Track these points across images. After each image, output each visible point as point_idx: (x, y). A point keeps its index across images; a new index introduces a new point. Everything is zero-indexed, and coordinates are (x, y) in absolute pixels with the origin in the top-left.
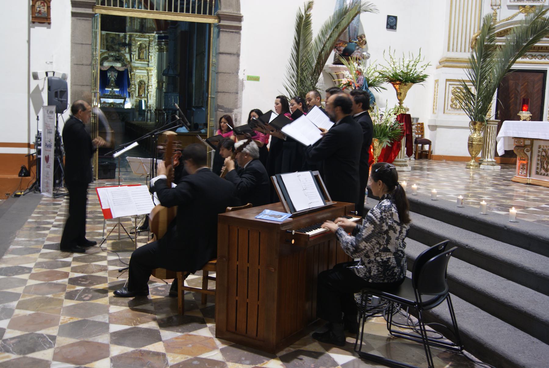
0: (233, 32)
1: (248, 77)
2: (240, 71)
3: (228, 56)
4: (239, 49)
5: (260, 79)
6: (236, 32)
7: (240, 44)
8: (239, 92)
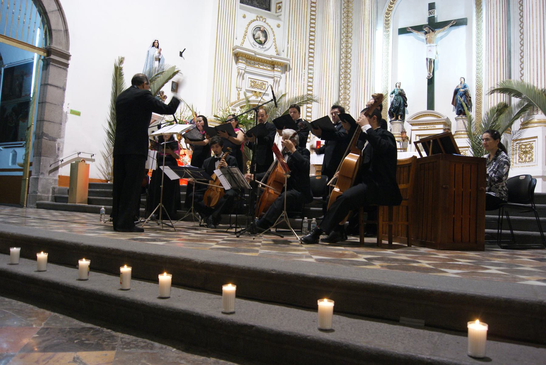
0: (61, 68)
2: (64, 104)
3: (55, 89)
4: (65, 84)
5: (81, 115)
6: (63, 69)
7: (66, 80)
8: (63, 123)
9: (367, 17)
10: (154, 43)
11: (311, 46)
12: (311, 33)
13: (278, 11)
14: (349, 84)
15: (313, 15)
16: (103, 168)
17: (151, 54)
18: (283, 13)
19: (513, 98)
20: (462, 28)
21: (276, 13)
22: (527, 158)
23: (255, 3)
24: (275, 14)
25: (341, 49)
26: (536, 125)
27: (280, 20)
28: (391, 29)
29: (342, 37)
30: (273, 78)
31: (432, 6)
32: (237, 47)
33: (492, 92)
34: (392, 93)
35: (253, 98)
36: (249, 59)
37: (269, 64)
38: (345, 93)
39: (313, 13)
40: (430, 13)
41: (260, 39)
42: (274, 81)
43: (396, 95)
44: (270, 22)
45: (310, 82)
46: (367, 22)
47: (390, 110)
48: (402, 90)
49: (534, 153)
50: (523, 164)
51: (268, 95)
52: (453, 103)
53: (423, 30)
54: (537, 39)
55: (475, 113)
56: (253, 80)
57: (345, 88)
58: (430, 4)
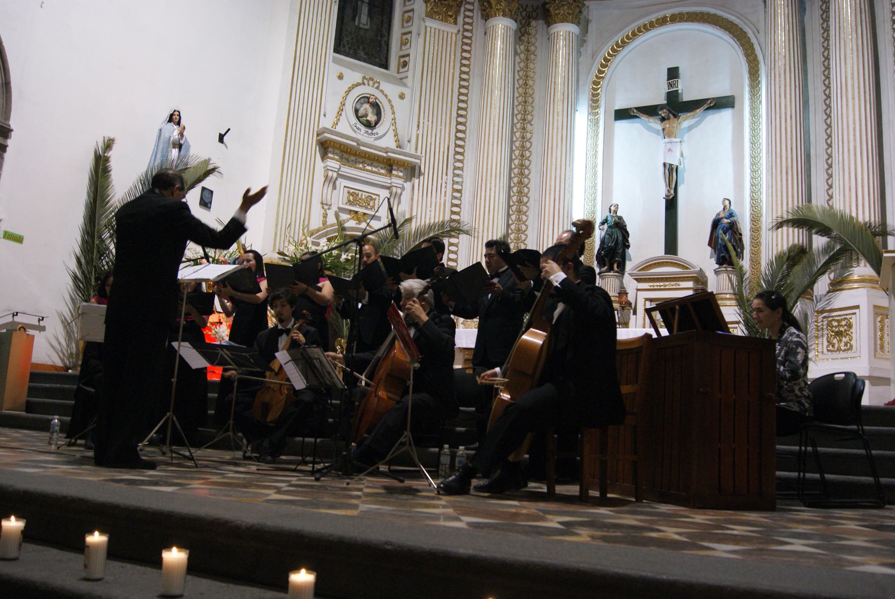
1: (6, 232)
5: (24, 241)
9: (560, 87)
10: (172, 115)
11: (460, 135)
12: (461, 112)
13: (401, 70)
14: (525, 204)
15: (464, 80)
16: (60, 343)
17: (166, 134)
18: (410, 74)
19: (815, 237)
20: (726, 114)
21: (398, 72)
22: (843, 344)
23: (362, 54)
24: (395, 74)
25: (512, 142)
26: (856, 285)
27: (405, 85)
28: (602, 111)
29: (515, 121)
30: (388, 188)
31: (673, 73)
32: (326, 130)
33: (780, 225)
34: (603, 223)
35: (352, 224)
36: (346, 152)
37: (383, 163)
38: (519, 220)
39: (464, 76)
40: (670, 85)
41: (368, 118)
42: (391, 193)
43: (610, 227)
44: (388, 90)
45: (456, 198)
46: (559, 95)
47: (599, 253)
48: (620, 218)
49: (854, 335)
50: (835, 355)
51: (379, 219)
52: (710, 244)
53: (657, 114)
54: (854, 135)
55: (748, 263)
56: (352, 191)
57: (519, 211)
58: (669, 70)
